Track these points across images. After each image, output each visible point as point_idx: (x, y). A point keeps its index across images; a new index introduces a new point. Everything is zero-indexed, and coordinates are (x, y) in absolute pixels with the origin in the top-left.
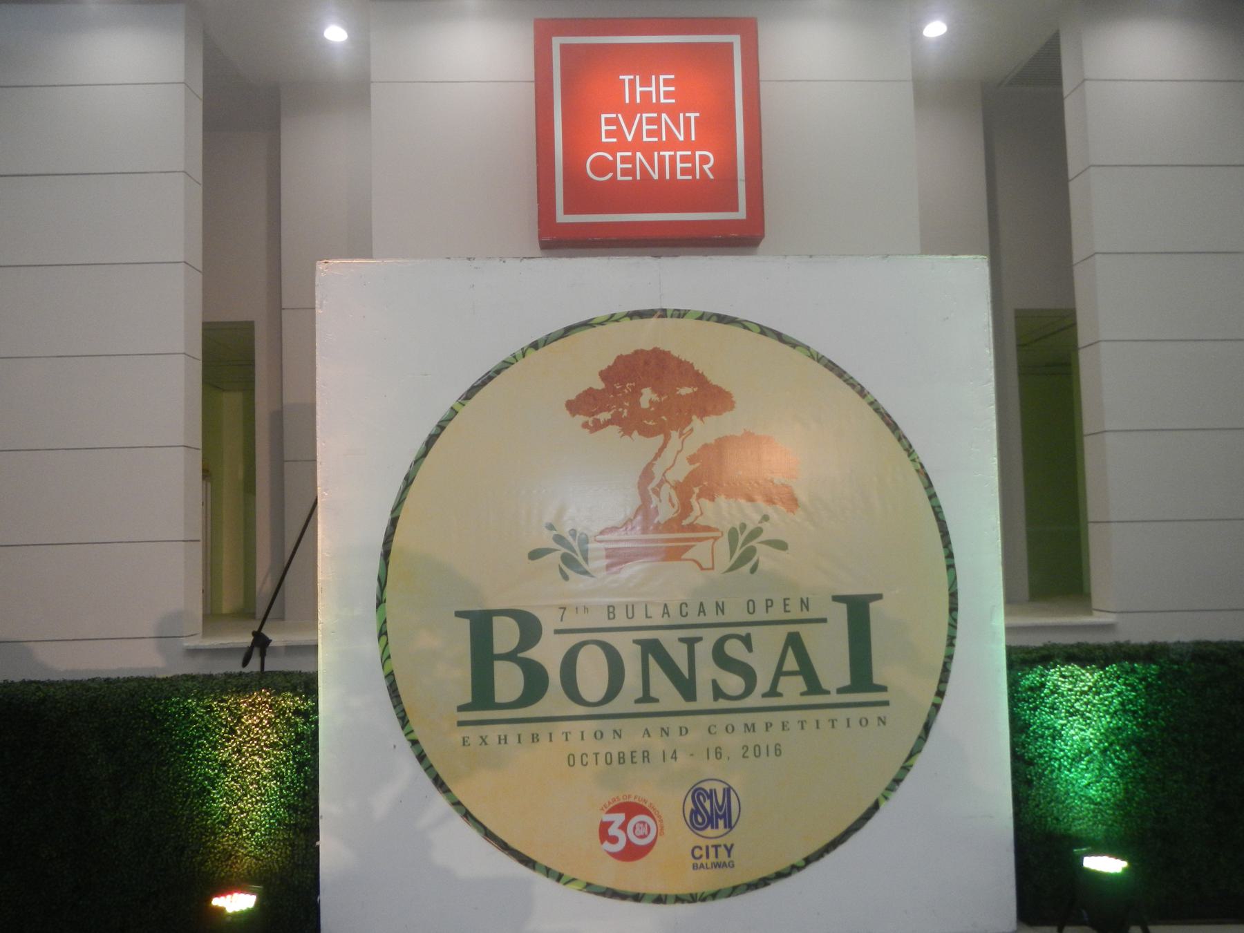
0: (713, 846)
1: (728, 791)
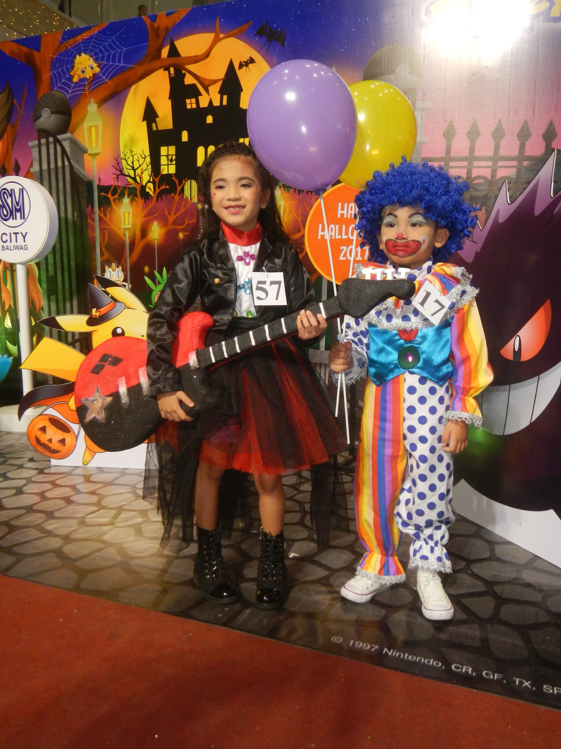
0: (14, 233)
1: (22, 190)
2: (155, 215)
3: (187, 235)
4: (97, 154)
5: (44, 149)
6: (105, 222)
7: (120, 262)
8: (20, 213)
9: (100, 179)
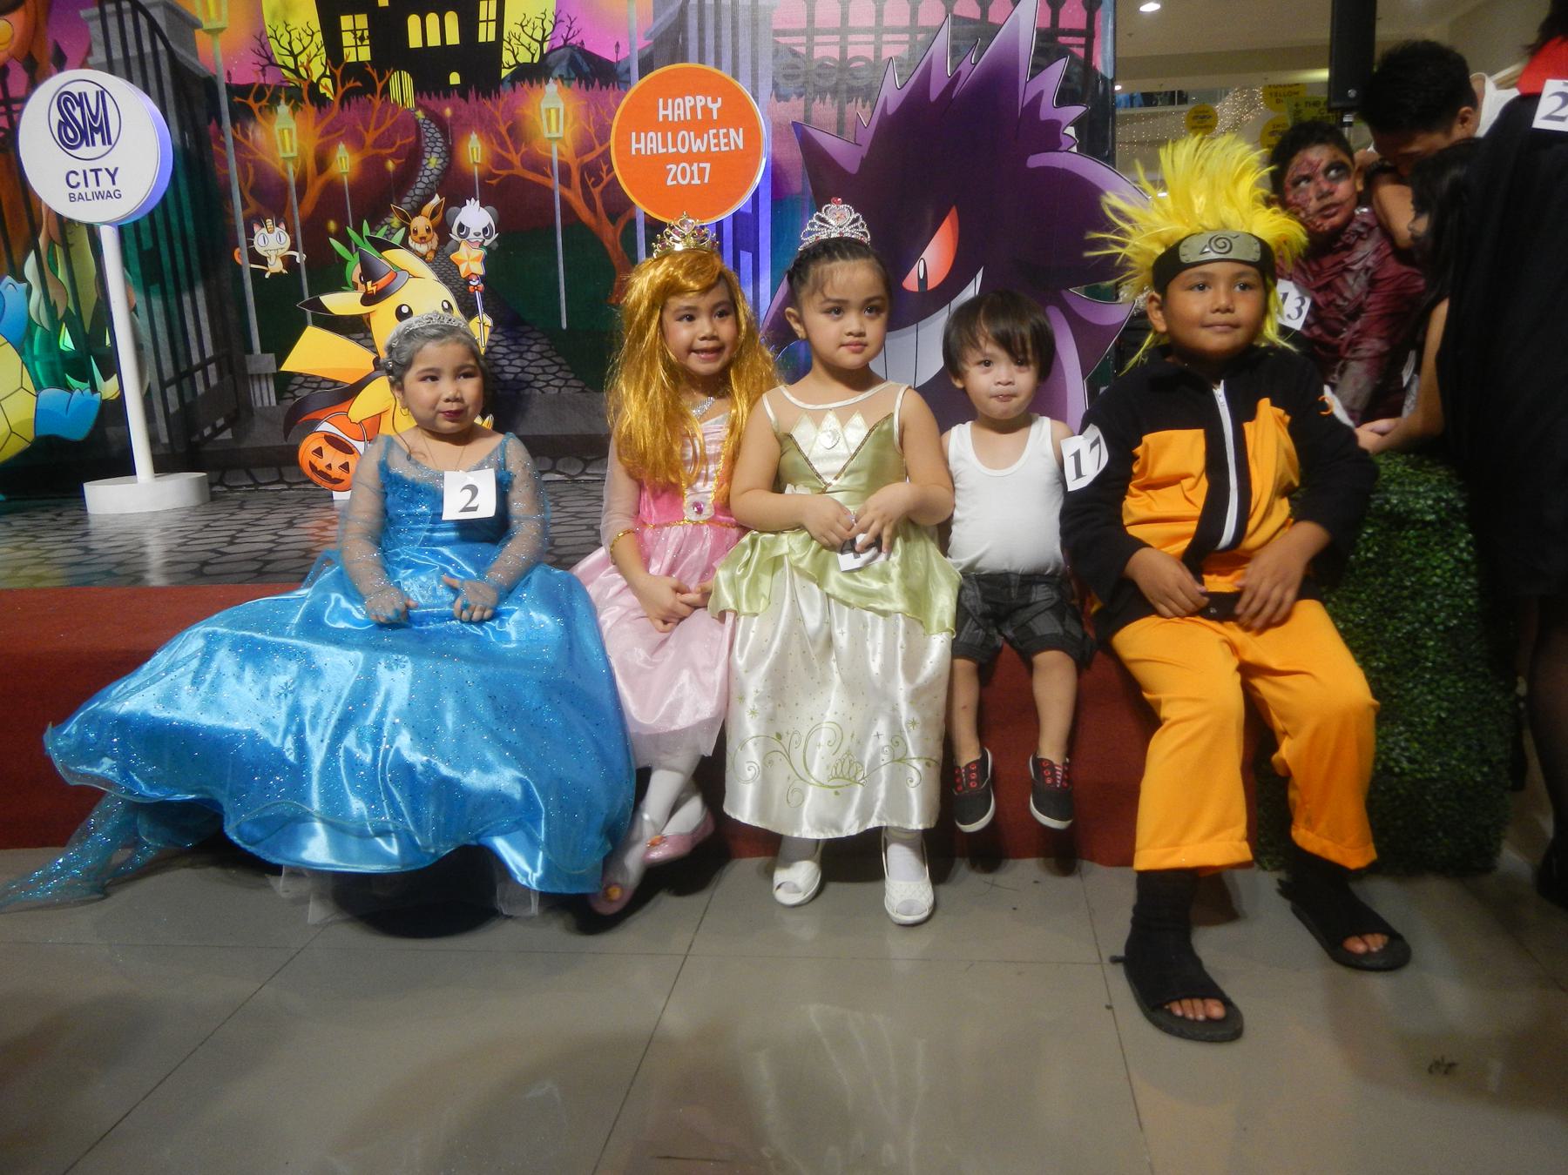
0: (92, 170)
1: (101, 95)
2: (339, 134)
3: (401, 164)
4: (220, 30)
5: (113, 23)
6: (246, 148)
7: (281, 216)
8: (100, 135)
9: (229, 74)
